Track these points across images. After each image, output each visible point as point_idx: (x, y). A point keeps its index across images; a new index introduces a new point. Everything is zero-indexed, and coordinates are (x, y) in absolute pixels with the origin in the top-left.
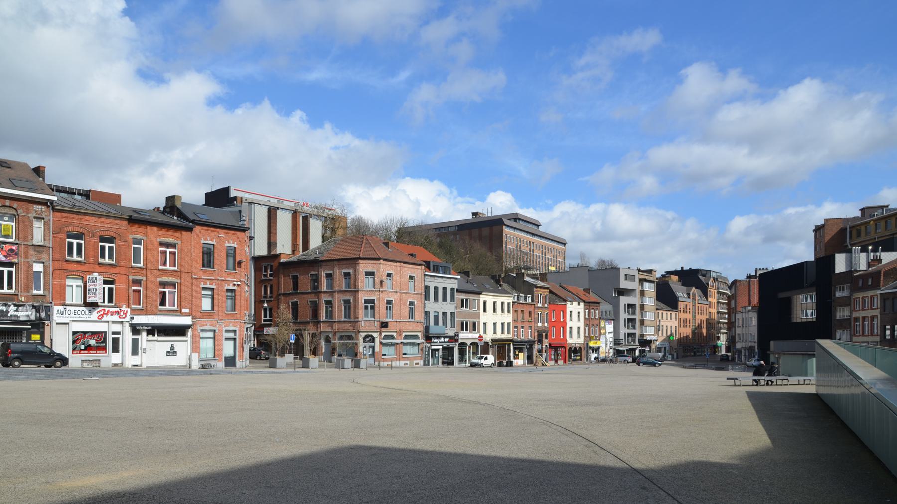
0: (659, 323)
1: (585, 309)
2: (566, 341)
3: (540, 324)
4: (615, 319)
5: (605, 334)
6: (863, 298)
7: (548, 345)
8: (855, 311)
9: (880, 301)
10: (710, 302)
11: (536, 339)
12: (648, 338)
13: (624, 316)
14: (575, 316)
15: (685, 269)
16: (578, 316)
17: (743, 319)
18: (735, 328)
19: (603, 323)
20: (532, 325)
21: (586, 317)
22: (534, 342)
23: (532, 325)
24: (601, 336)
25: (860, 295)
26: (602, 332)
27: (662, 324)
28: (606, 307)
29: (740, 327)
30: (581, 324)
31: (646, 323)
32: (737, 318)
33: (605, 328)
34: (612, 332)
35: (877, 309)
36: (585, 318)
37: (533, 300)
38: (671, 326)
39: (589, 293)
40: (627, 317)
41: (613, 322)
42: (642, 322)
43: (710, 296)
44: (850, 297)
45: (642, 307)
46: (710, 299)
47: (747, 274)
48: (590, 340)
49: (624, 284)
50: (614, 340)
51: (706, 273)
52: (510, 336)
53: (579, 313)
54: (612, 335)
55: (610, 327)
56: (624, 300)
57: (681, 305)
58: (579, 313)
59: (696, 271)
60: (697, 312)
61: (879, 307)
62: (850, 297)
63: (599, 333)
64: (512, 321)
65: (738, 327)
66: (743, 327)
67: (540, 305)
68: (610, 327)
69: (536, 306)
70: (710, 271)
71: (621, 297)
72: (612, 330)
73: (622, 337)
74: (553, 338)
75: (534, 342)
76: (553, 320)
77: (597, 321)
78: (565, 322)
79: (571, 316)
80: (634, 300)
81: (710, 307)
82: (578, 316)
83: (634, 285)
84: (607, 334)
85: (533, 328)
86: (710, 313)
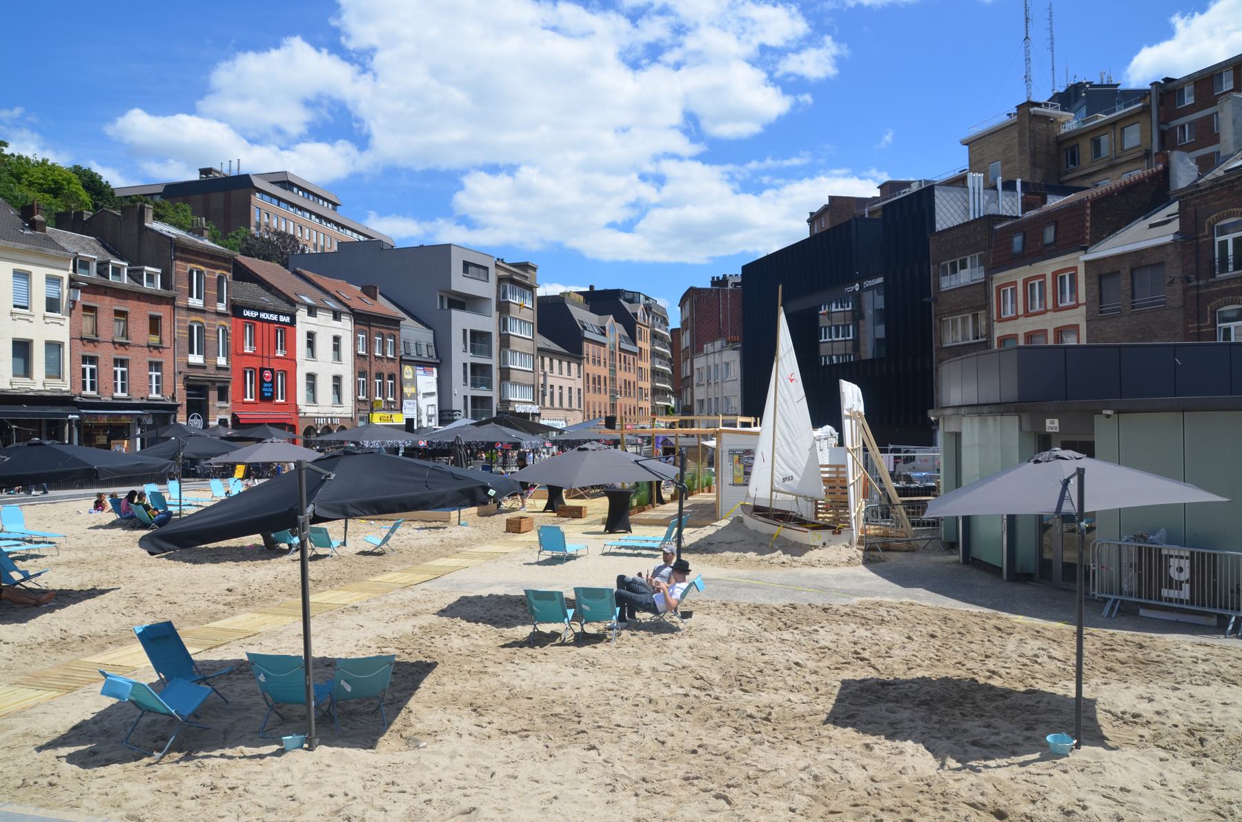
0: (545, 380)
1: (356, 332)
2: (297, 411)
3: (196, 359)
4: (439, 361)
5: (415, 396)
6: (1025, 282)
7: (229, 418)
8: (1000, 320)
9: (1087, 284)
10: (641, 349)
11: (182, 399)
12: (520, 409)
13: (461, 356)
14: (324, 345)
15: (596, 289)
16: (337, 348)
17: (709, 367)
18: (692, 388)
19: (408, 371)
20: (166, 358)
21: (360, 352)
22: (174, 408)
23: (166, 358)
24: (405, 402)
25: (1019, 275)
26: (408, 390)
27: (550, 381)
28: (414, 333)
29: (703, 385)
30: (346, 369)
31: (514, 376)
32: (695, 367)
33: (414, 382)
34: (432, 394)
35: (1077, 306)
36: (357, 356)
37: (166, 284)
38: (570, 388)
39: (374, 298)
40: (470, 358)
41: (435, 370)
42: (505, 373)
43: (641, 339)
44: (986, 285)
45: (505, 341)
46: (640, 343)
47: (713, 278)
48: (372, 410)
49: (461, 284)
50: (440, 412)
51: (633, 298)
52: (64, 386)
53: (337, 339)
54: (434, 400)
55: (427, 381)
56: (462, 321)
57: (588, 348)
58: (337, 339)
59: (617, 293)
60: (618, 364)
61: (1082, 299)
62: (986, 285)
63: (398, 393)
64: (71, 339)
65: (698, 385)
66: (709, 384)
67: (195, 302)
68: (427, 381)
69: (179, 303)
70: (639, 293)
71: (456, 314)
72: (434, 389)
73: (457, 404)
74: (248, 399)
75: (174, 408)
76: (247, 350)
77: (391, 364)
78: (291, 360)
79: (311, 344)
80: (488, 323)
81: (641, 359)
82: (337, 348)
83: (486, 289)
84: (420, 397)
85: (168, 367)
86: (641, 368)
